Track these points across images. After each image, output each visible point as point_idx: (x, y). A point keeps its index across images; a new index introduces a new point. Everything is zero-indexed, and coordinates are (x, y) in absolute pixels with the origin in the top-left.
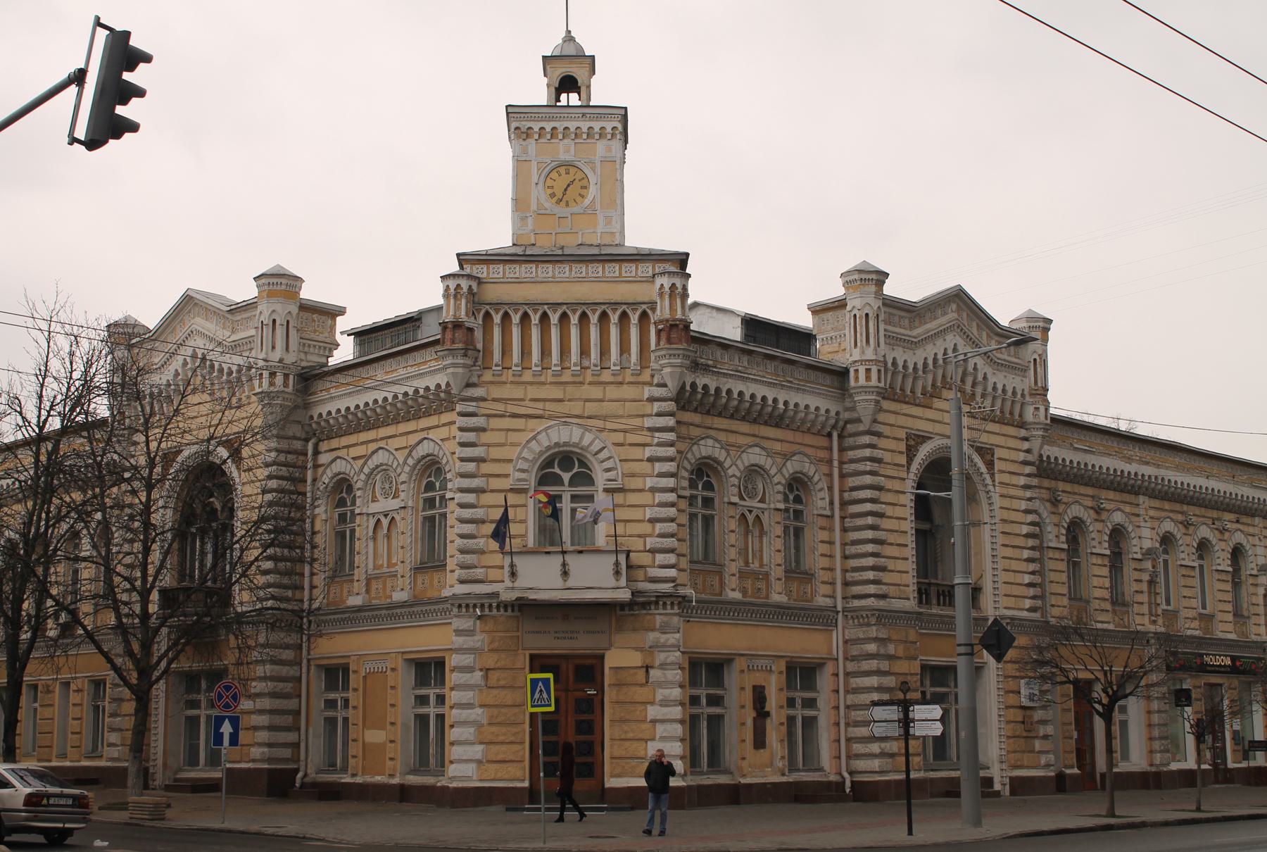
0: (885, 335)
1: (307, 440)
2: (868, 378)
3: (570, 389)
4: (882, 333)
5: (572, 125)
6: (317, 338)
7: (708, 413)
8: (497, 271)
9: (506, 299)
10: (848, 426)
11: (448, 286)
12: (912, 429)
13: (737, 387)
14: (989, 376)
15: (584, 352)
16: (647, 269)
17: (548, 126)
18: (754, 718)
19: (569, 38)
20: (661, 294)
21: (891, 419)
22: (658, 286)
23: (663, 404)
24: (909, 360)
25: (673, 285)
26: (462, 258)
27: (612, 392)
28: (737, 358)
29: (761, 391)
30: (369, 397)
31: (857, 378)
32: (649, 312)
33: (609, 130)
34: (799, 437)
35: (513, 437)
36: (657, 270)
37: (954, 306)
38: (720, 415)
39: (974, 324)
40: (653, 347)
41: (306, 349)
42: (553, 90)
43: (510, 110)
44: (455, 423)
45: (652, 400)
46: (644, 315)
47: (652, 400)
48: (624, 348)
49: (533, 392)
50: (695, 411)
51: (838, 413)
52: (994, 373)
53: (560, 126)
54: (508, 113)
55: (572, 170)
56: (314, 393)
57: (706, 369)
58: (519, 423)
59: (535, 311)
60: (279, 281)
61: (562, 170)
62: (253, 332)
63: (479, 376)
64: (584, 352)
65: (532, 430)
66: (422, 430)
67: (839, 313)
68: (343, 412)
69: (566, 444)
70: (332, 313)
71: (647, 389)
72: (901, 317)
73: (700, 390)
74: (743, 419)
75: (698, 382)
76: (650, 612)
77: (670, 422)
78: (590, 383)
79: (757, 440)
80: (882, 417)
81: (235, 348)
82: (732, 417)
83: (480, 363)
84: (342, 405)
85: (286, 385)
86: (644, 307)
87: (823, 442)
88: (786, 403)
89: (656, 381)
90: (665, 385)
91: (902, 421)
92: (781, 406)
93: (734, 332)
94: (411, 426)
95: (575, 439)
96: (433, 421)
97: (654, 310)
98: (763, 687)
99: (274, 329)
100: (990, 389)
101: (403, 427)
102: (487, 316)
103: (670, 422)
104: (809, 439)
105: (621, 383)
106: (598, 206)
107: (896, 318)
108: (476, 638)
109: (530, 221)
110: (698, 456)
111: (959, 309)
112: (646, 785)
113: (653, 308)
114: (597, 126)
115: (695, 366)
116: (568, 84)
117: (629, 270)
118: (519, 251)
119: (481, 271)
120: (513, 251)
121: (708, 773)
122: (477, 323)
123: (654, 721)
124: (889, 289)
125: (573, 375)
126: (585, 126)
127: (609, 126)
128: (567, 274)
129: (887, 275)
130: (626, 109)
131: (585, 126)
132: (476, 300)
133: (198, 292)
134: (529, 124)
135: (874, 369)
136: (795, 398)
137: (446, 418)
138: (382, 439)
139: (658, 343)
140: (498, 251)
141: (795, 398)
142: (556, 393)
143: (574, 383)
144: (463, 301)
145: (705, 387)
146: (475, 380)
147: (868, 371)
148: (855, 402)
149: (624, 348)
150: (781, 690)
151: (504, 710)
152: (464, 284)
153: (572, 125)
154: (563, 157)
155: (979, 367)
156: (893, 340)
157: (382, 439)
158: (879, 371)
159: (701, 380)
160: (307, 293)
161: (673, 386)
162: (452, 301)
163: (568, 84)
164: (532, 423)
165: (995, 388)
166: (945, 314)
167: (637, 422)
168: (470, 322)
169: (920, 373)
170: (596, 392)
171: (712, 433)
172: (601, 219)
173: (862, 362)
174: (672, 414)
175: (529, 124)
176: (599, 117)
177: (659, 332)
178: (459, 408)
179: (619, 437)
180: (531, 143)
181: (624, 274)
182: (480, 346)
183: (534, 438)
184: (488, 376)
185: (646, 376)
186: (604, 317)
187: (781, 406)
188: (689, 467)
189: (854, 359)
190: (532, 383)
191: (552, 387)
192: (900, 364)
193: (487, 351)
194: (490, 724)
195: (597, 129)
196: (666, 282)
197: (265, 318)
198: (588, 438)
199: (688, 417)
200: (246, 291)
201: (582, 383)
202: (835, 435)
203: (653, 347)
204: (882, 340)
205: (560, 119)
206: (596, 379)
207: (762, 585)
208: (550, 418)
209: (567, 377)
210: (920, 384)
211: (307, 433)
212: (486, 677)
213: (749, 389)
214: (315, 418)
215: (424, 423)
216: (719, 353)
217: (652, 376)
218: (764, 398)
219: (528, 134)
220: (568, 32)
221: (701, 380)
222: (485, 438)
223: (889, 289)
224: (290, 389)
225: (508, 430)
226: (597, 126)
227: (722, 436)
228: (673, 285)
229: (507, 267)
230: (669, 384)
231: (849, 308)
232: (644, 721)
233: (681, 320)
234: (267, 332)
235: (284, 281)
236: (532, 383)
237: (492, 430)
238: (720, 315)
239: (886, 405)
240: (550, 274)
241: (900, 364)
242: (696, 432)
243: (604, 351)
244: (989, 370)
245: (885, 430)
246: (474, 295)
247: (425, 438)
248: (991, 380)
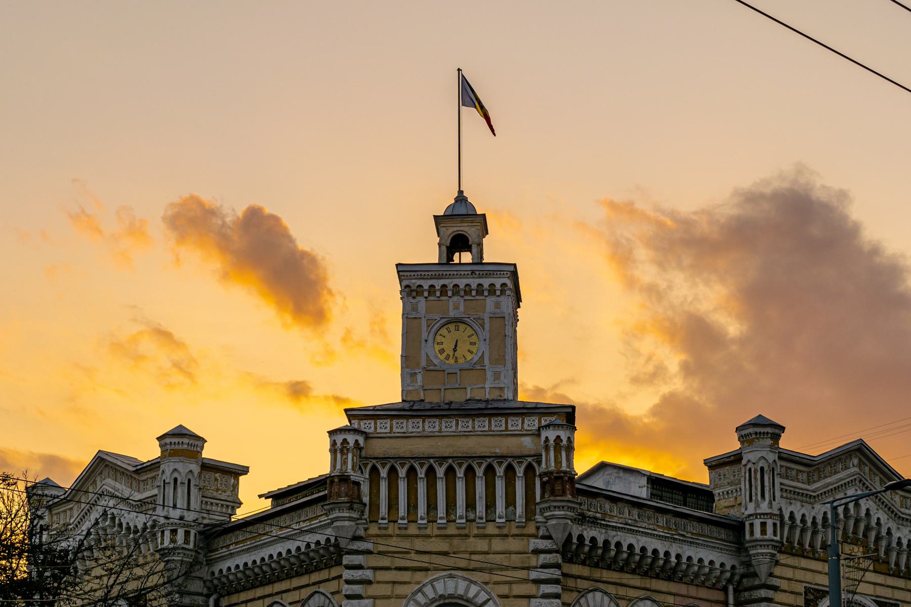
0: (782, 489)
1: (208, 596)
2: (764, 532)
3: (456, 541)
4: (777, 487)
5: (462, 283)
6: (219, 497)
7: (596, 566)
8: (383, 426)
9: (392, 453)
10: (745, 580)
11: (335, 441)
12: (811, 583)
13: (627, 539)
14: (893, 531)
15: (471, 505)
16: (532, 423)
17: (438, 284)
19: (461, 198)
20: (547, 448)
21: (789, 573)
22: (543, 438)
23: (548, 556)
24: (807, 515)
25: (558, 437)
26: (351, 413)
27: (498, 545)
28: (626, 511)
29: (652, 544)
30: (265, 553)
31: (752, 533)
32: (535, 465)
33: (498, 286)
34: (693, 591)
35: (400, 590)
36: (543, 423)
37: (856, 461)
38: (609, 568)
39: (877, 478)
40: (538, 499)
41: (209, 507)
42: (444, 249)
43: (401, 268)
44: (340, 577)
46: (530, 469)
47: (537, 552)
48: (510, 501)
49: (419, 545)
50: (583, 563)
51: (733, 567)
52: (899, 528)
53: (450, 283)
54: (398, 272)
55: (462, 326)
56: (217, 550)
57: (594, 522)
58: (406, 576)
59: (422, 465)
60: (181, 440)
61: (452, 327)
62: (155, 491)
63: (366, 529)
64: (471, 505)
65: (418, 583)
66: (314, 584)
67: (735, 468)
68: (241, 568)
69: (451, 596)
70: (236, 472)
71: (533, 540)
72: (799, 471)
73: (587, 542)
74: (633, 572)
75: (585, 534)
77: (555, 573)
78: (476, 536)
79: (649, 594)
80: (778, 571)
81: (142, 506)
82: (621, 570)
83: (366, 516)
84: (240, 561)
85: (187, 541)
86: (530, 459)
87: (720, 596)
88: (678, 557)
89: (541, 533)
90: (549, 537)
91: (799, 575)
92: (673, 559)
93: (640, 490)
94: (304, 580)
95: (461, 592)
96: (324, 575)
97: (539, 463)
99: (175, 488)
100: (894, 544)
101: (296, 582)
102: (374, 471)
103: (555, 573)
104: (703, 593)
105: (506, 536)
106: (486, 362)
107: (794, 473)
109: (419, 377)
111: (861, 464)
113: (538, 458)
114: (486, 282)
115: (582, 519)
116: (458, 243)
117: (515, 424)
118: (407, 406)
119: (368, 426)
120: (400, 406)
122: (363, 478)
124: (785, 443)
125: (458, 528)
126: (474, 283)
127: (498, 283)
128: (454, 428)
129: (783, 429)
130: (515, 265)
131: (474, 283)
132: (363, 454)
133: (107, 454)
134: (419, 282)
135: (770, 523)
136: (688, 551)
137: (335, 572)
138: (277, 593)
139: (542, 496)
140: (390, 407)
141: (688, 551)
142: (443, 546)
143: (459, 535)
144: (350, 455)
145: (593, 540)
146: (361, 532)
147: (763, 525)
148: (750, 556)
149: (510, 501)
152: (351, 439)
153: (462, 283)
154: (452, 314)
155: (882, 522)
156: (792, 494)
157: (277, 593)
158: (775, 525)
159: (589, 533)
160: (208, 453)
161: (560, 537)
162: (339, 455)
163: (458, 243)
164: (419, 576)
165: (899, 543)
166: (847, 468)
167: (522, 574)
168: (355, 476)
169: (820, 527)
170: (482, 545)
171: (601, 586)
172: (489, 374)
173: (756, 515)
174: (557, 566)
175: (419, 282)
176: (488, 274)
177: (543, 485)
178: (347, 560)
180: (422, 303)
181: (510, 428)
182: (366, 500)
183: (420, 590)
184: (374, 530)
185: (531, 529)
186: (490, 470)
187: (673, 559)
189: (747, 513)
190: (417, 536)
191: (438, 539)
192: (798, 518)
193: (374, 506)
195: (486, 286)
196: (551, 434)
197: (168, 477)
198: (474, 590)
199: (576, 569)
200: (149, 452)
201: (467, 536)
202: (731, 588)
203: (538, 499)
204: (778, 494)
205: (449, 277)
206: (481, 531)
208: (436, 569)
209: (451, 530)
210: (819, 537)
211: (209, 588)
213: (639, 541)
214: (217, 575)
215: (315, 577)
216: (607, 505)
217: (538, 528)
218: (655, 552)
219: (419, 291)
220: (461, 192)
221: (589, 533)
222: (372, 590)
223: (785, 443)
224: (191, 546)
225: (394, 583)
226: (486, 282)
227: (611, 589)
228: (558, 437)
229: (394, 422)
230: (554, 536)
231: (744, 462)
233: (565, 472)
234: (170, 490)
235: (186, 440)
236: (417, 536)
237: (379, 582)
238: (627, 476)
239: (782, 558)
240: (437, 428)
241: (798, 518)
242: (583, 584)
243: (490, 505)
244: (893, 525)
245: (784, 585)
246: (361, 449)
247: (316, 592)
248: (896, 535)
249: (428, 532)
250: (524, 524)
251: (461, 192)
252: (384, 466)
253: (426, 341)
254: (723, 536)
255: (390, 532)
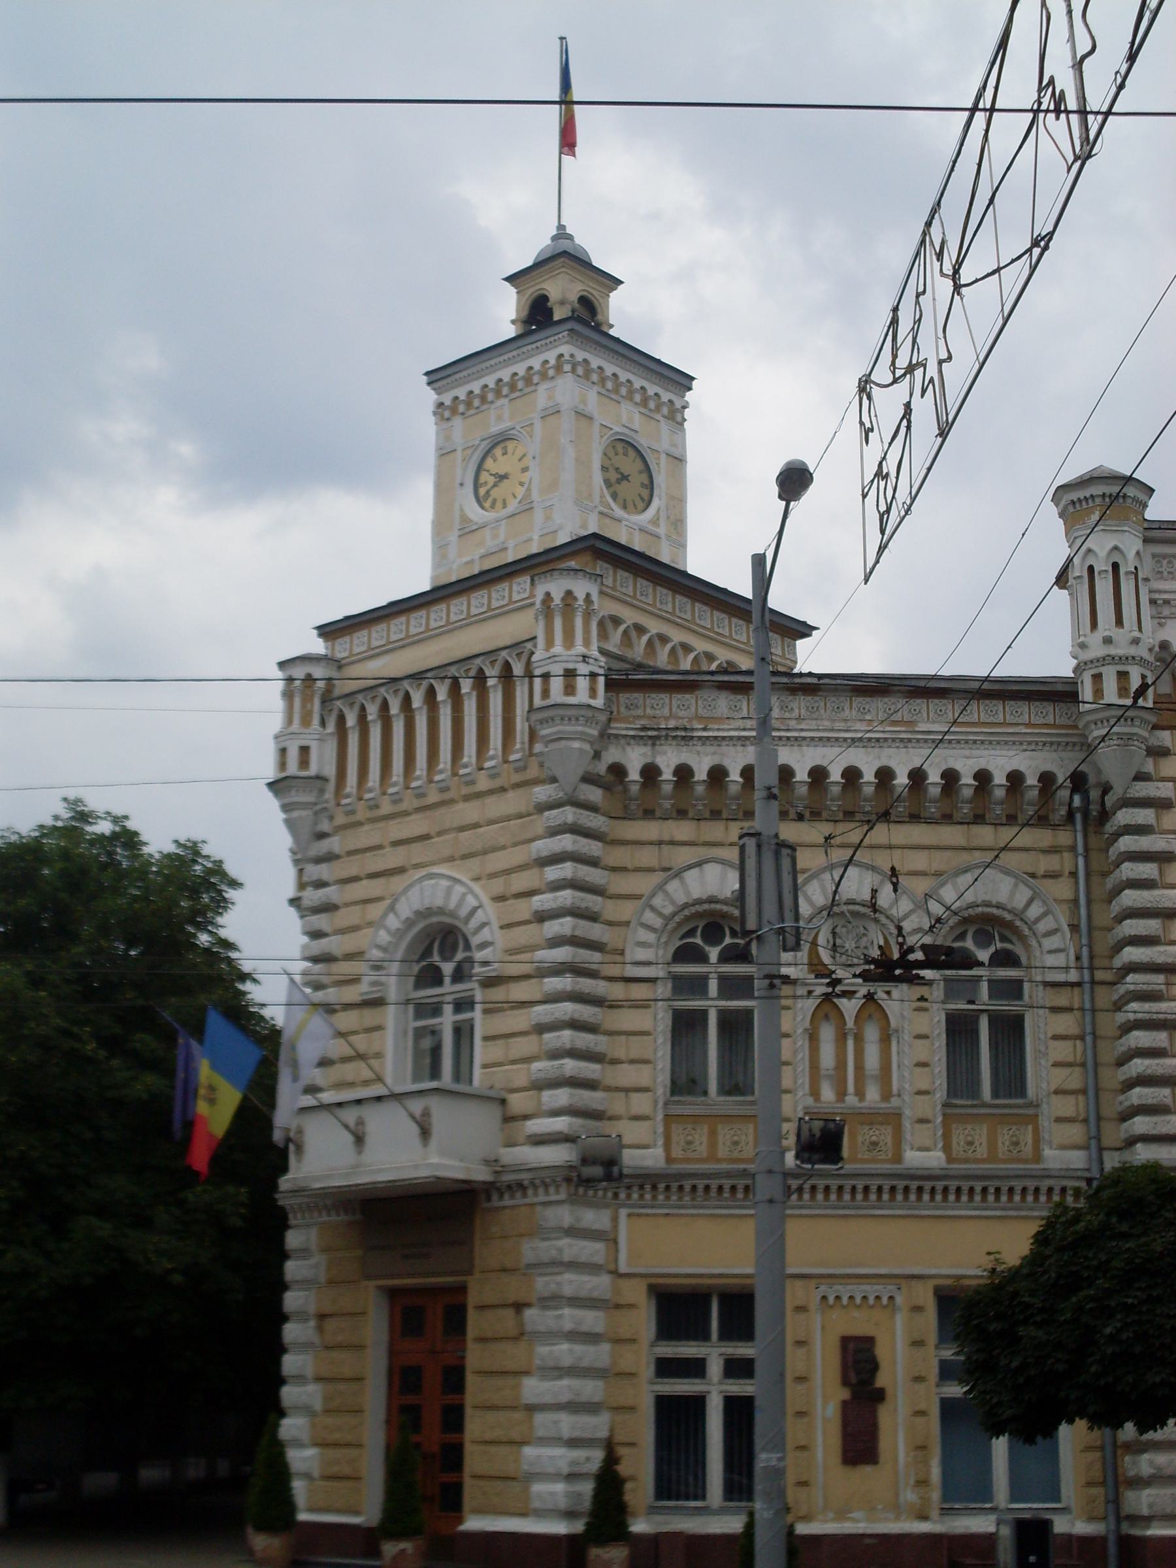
18: (845, 1404)
19: (562, 234)
45: (542, 808)
47: (542, 808)
55: (510, 445)
57: (684, 737)
63: (331, 818)
75: (661, 761)
76: (527, 1201)
98: (870, 1341)
108: (313, 1261)
110: (681, 899)
112: (462, 1528)
119: (342, 648)
121: (722, 1511)
123: (531, 1409)
147: (1097, 678)
150: (918, 1343)
151: (341, 1387)
170: (470, 812)
179: (498, 886)
186: (480, 679)
188: (657, 922)
194: (327, 1411)
207: (885, 1136)
212: (320, 1329)
220: (561, 227)
222: (343, 918)
230: (558, 773)
232: (513, 1408)
242: (684, 856)
249: (404, 806)
250: (521, 764)
251: (561, 227)
252: (352, 705)
253: (462, 485)
254: (1050, 719)
255: (360, 815)
